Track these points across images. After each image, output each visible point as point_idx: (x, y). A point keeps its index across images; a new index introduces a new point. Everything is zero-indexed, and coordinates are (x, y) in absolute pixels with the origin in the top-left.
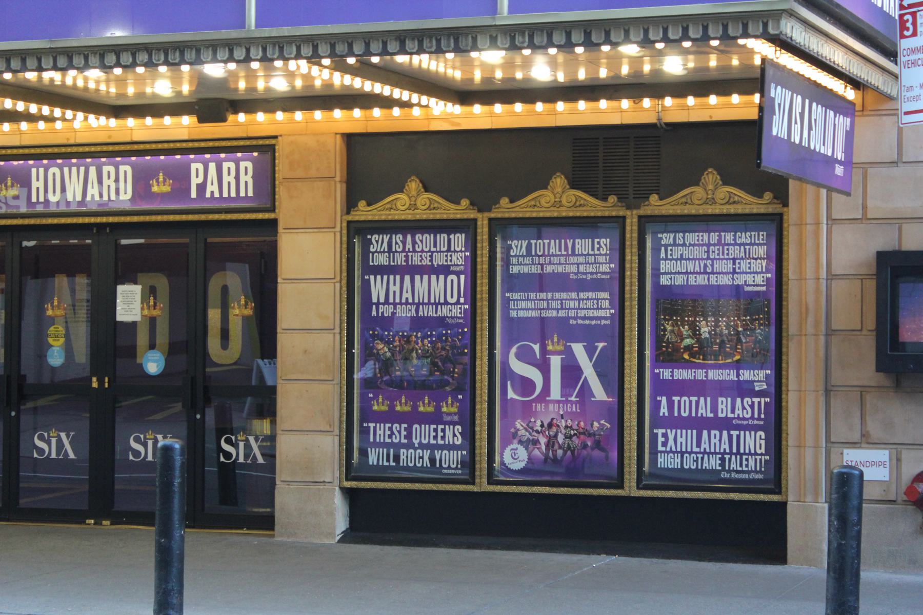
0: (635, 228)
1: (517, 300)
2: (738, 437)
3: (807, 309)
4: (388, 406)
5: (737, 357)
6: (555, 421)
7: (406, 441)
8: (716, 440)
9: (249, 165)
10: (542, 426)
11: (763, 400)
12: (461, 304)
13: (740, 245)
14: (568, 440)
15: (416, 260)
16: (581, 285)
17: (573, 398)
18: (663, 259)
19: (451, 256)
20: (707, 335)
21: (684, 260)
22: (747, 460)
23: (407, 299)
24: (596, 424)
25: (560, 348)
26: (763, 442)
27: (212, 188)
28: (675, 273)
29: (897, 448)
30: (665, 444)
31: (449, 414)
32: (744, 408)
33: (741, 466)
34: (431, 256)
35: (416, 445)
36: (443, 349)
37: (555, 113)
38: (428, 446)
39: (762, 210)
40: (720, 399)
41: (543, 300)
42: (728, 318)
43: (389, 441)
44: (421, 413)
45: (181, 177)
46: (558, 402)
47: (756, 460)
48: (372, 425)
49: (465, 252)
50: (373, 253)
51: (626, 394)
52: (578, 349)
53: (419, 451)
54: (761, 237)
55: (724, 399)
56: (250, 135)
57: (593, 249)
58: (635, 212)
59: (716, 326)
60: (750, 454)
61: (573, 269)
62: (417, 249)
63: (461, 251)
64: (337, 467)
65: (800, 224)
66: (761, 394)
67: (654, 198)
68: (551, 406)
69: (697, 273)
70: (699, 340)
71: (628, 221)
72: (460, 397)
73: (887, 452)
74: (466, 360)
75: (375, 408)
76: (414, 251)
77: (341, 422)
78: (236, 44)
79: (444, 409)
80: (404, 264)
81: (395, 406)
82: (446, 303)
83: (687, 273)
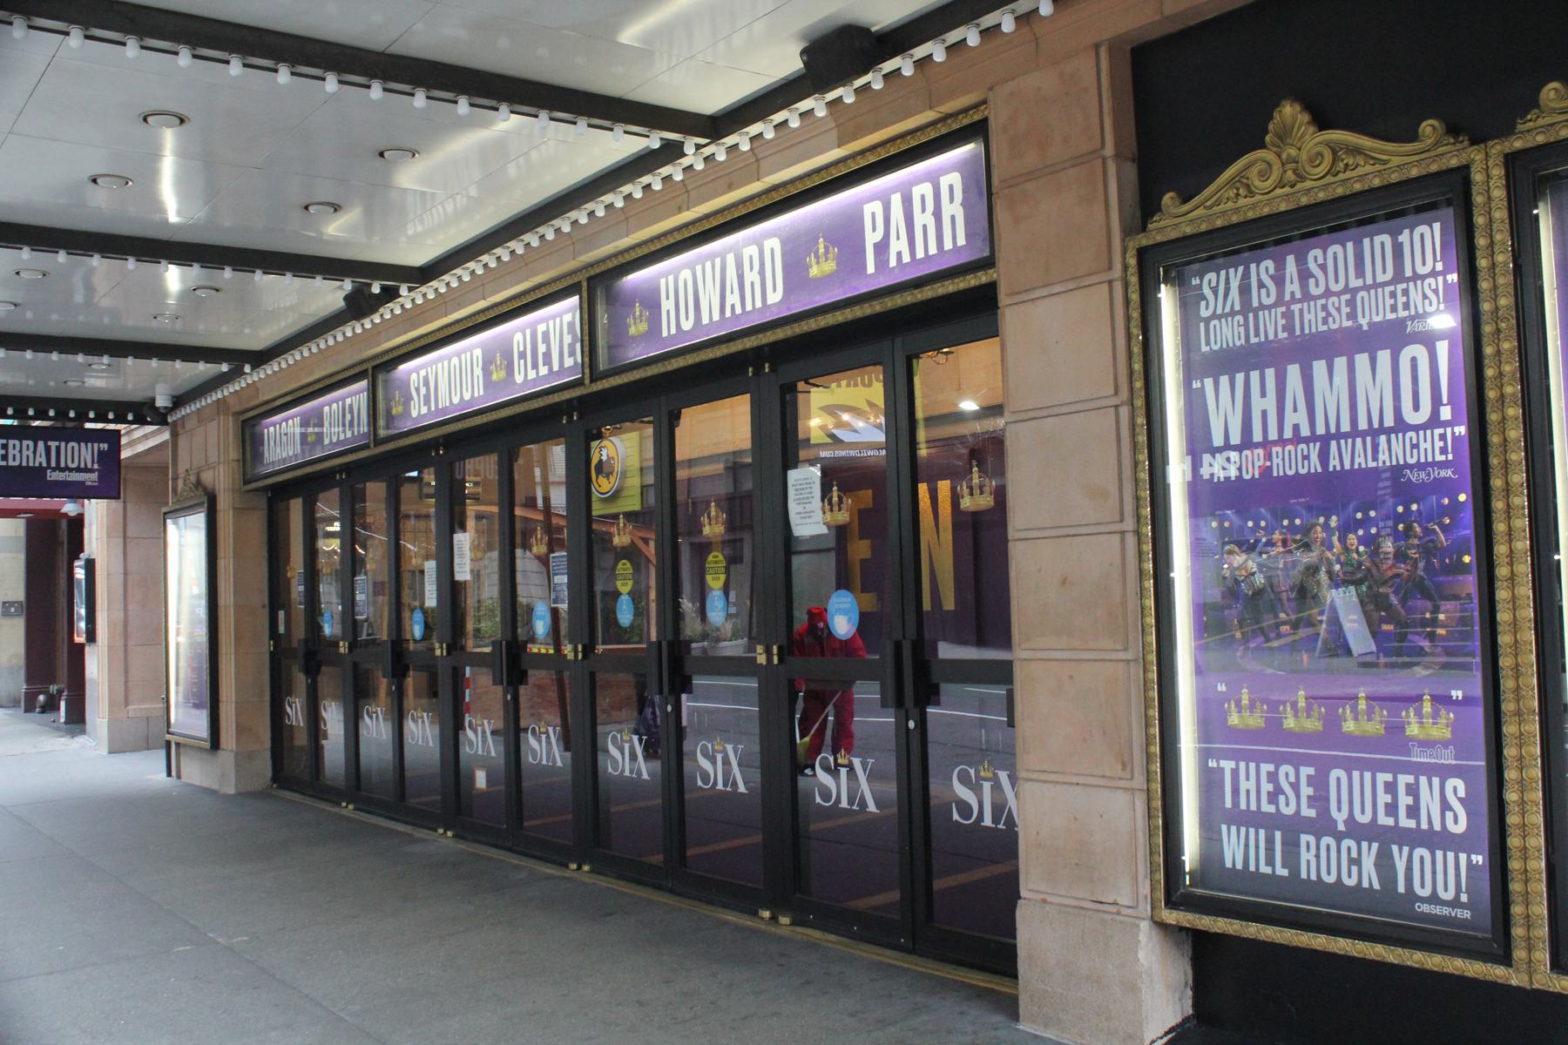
12: (1445, 424)
15: (1312, 319)
19: (1406, 292)
23: (1296, 427)
27: (899, 245)
31: (1427, 744)
34: (1351, 303)
35: (1341, 827)
36: (1400, 556)
43: (1271, 809)
45: (846, 236)
49: (1444, 273)
50: (1207, 321)
62: (1314, 291)
63: (1434, 274)
64: (1143, 869)
74: (1469, 584)
76: (1307, 297)
77: (1149, 757)
79: (1413, 730)
80: (1283, 335)
82: (1401, 426)
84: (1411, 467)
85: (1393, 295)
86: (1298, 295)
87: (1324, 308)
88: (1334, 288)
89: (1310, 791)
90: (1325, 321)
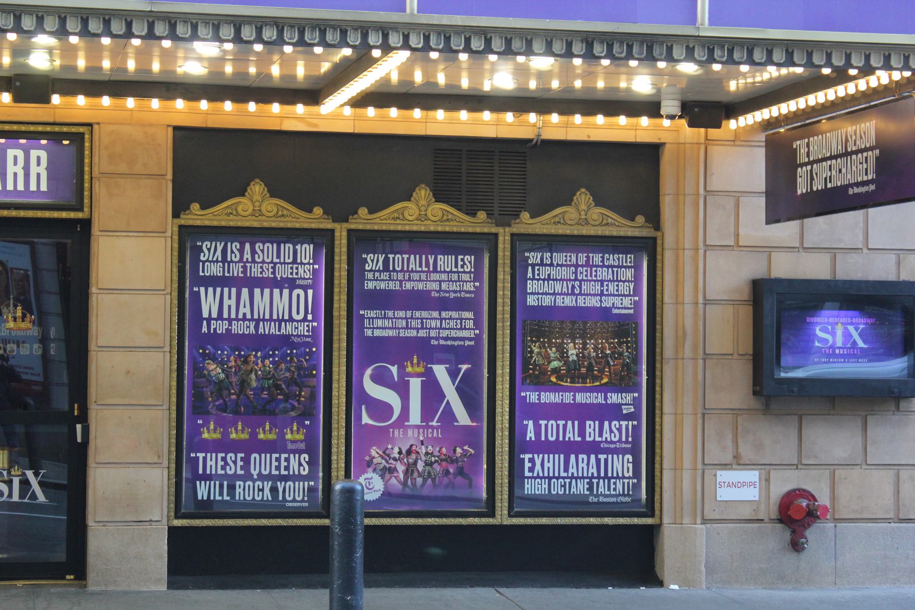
0: (508, 246)
1: (373, 318)
2: (606, 460)
3: (685, 333)
4: (250, 434)
5: (605, 380)
6: (414, 448)
7: (242, 472)
8: (583, 464)
9: (43, 154)
10: (400, 453)
11: (630, 423)
12: (309, 321)
13: (608, 267)
14: (428, 468)
15: (255, 271)
16: (444, 304)
17: (434, 423)
18: (530, 279)
19: (297, 268)
20: (575, 358)
21: (553, 284)
22: (615, 483)
23: (245, 314)
24: (459, 450)
25: (420, 369)
26: (631, 465)
28: (542, 294)
29: (766, 468)
30: (531, 470)
31: (293, 442)
32: (611, 431)
33: (609, 490)
34: (274, 268)
35: (255, 477)
37: (567, 126)
38: (269, 477)
39: (637, 233)
40: (588, 423)
41: (402, 318)
42: (596, 340)
44: (261, 441)
46: (418, 427)
47: (624, 483)
48: (201, 455)
49: (313, 264)
50: (204, 262)
51: (498, 418)
52: (440, 372)
53: (260, 483)
54: (629, 260)
55: (592, 423)
56: (58, 120)
57: (456, 266)
58: (507, 229)
59: (584, 348)
60: (618, 477)
61: (435, 286)
62: (257, 259)
63: (309, 264)
65: (676, 249)
66: (628, 417)
67: (525, 216)
68: (410, 432)
69: (565, 294)
70: (566, 363)
71: (501, 238)
72: (307, 423)
73: (757, 473)
75: (206, 435)
76: (254, 261)
78: (391, 28)
79: (289, 436)
80: (241, 275)
81: (257, 434)
82: (291, 319)
83: (554, 294)
84: (295, 336)
85: (292, 268)
86: (250, 260)
87: (261, 267)
88: (266, 260)
89: (242, 463)
90: (261, 273)
